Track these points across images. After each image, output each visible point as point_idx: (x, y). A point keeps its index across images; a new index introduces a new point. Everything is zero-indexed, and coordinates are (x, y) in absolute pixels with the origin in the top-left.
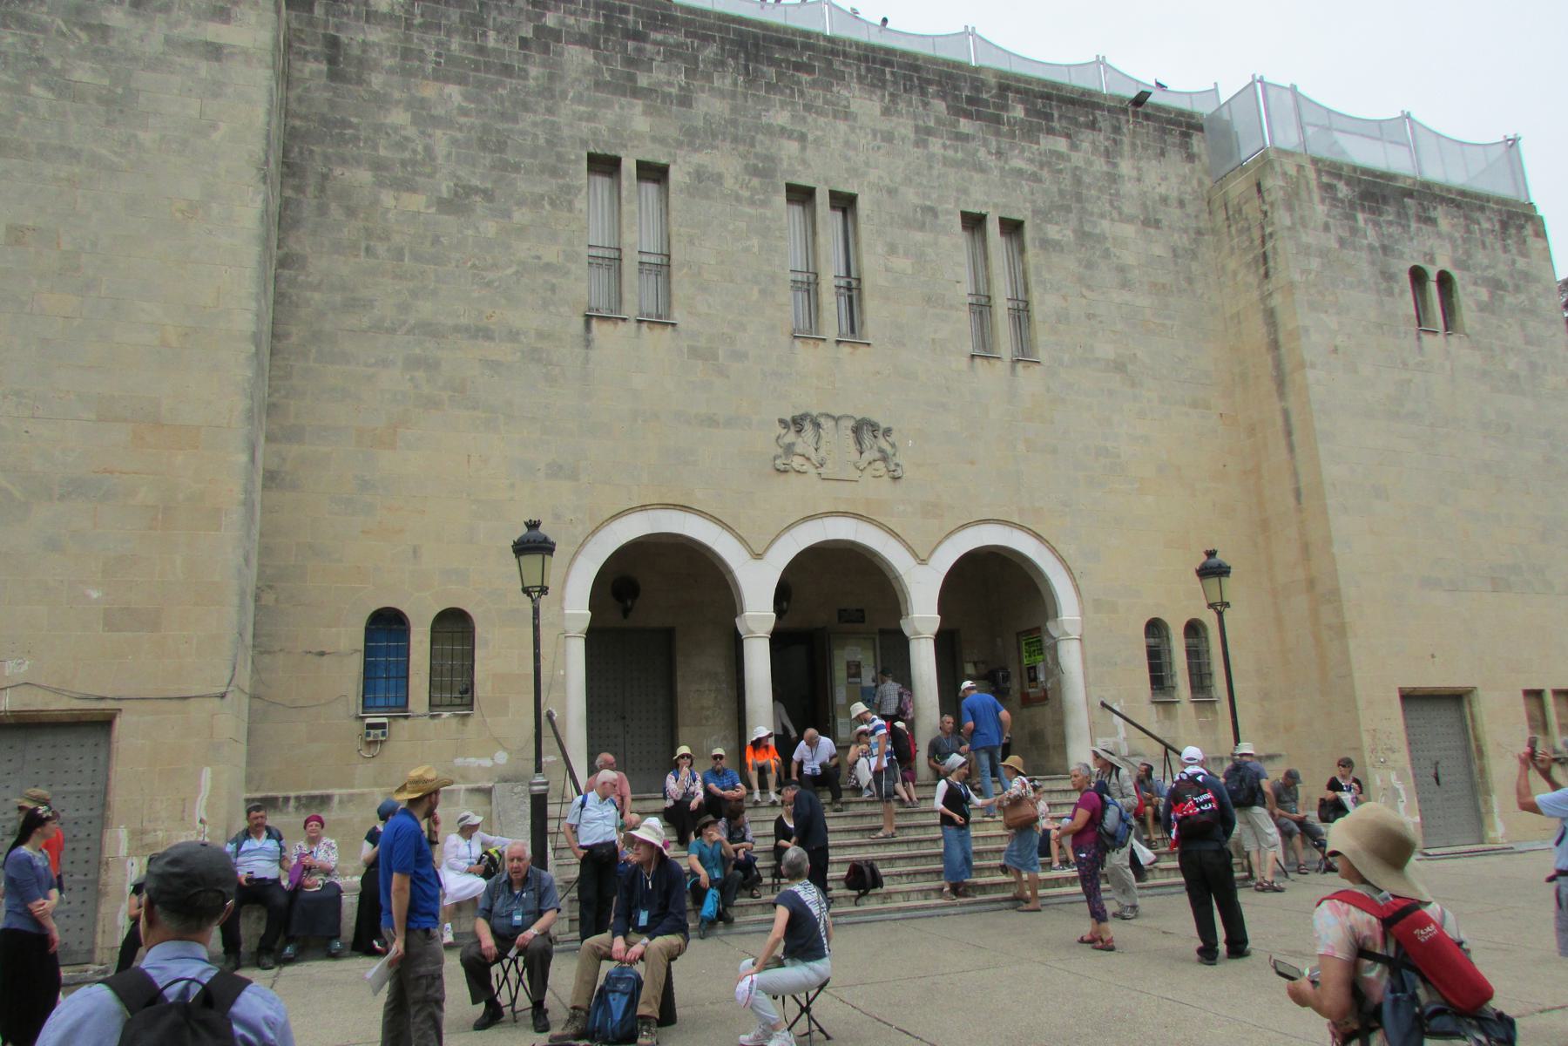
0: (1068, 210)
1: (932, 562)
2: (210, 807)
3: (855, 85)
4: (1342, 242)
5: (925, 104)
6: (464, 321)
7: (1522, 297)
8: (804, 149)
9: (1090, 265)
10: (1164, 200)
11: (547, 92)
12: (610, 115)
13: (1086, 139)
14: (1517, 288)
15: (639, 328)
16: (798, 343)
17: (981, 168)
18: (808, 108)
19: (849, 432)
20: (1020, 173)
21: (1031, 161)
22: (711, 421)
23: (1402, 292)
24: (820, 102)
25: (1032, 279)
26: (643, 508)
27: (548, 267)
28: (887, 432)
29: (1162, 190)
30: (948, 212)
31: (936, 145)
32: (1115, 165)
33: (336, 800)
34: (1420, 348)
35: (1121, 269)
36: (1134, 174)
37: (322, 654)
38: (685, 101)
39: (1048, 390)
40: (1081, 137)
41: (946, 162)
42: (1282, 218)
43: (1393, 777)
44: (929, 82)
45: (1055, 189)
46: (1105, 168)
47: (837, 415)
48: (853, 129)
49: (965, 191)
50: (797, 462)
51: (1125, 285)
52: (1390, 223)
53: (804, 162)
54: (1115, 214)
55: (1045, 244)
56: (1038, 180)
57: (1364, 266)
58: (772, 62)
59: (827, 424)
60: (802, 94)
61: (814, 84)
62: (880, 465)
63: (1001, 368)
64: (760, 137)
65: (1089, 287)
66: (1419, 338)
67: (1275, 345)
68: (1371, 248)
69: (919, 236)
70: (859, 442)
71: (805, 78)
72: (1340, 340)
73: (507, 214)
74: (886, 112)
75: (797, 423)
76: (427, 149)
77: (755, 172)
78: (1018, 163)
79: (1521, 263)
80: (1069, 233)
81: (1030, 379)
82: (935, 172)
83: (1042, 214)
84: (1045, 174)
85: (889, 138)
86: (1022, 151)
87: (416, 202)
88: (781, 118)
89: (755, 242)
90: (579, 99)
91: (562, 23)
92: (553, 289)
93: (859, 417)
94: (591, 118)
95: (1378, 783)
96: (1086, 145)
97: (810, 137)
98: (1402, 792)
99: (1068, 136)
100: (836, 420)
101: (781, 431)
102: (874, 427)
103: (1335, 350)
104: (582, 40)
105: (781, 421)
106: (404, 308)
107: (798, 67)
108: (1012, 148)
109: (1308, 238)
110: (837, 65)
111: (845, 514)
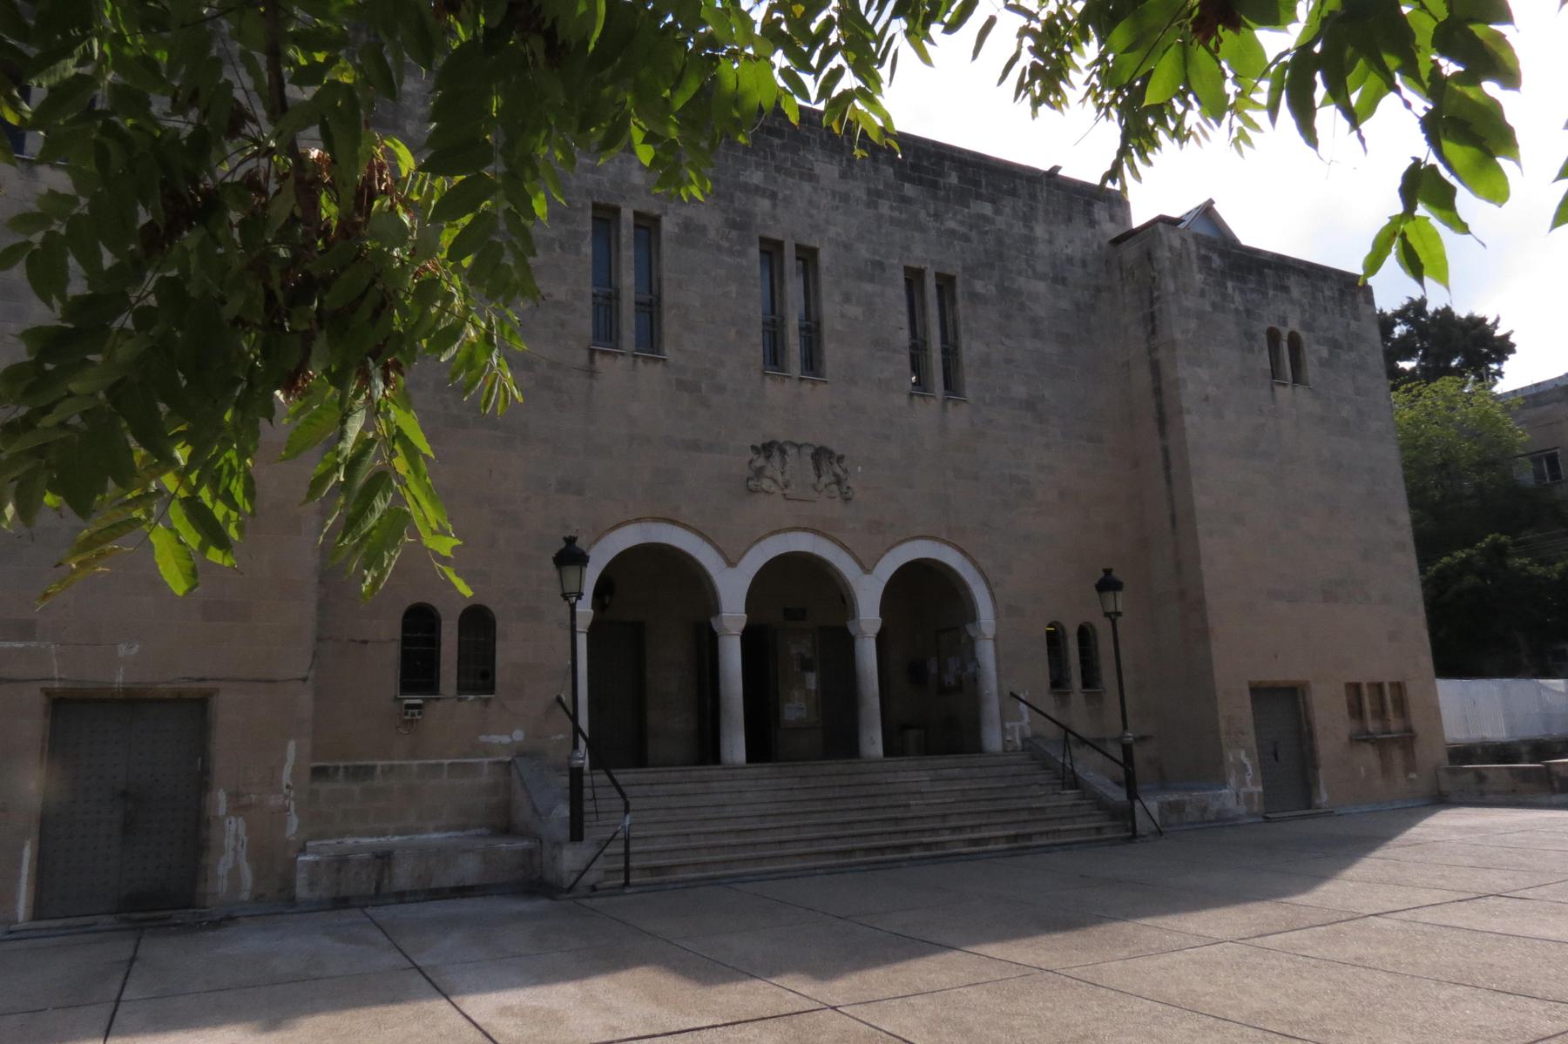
1: (875, 571)
2: (294, 776)
3: (817, 149)
4: (1214, 305)
5: (876, 170)
7: (1353, 354)
8: (774, 206)
10: (1070, 260)
13: (1007, 203)
14: (1351, 348)
15: (635, 363)
16: (768, 380)
17: (922, 229)
18: (778, 169)
19: (809, 459)
20: (953, 232)
21: (962, 223)
22: (695, 446)
23: (1261, 349)
24: (789, 164)
25: (962, 327)
26: (638, 520)
28: (841, 459)
29: (1069, 251)
31: (885, 208)
32: (1032, 229)
33: (379, 769)
34: (1274, 398)
35: (1034, 320)
36: (1047, 237)
37: (365, 642)
41: (893, 221)
42: (1169, 285)
46: (1023, 231)
47: (799, 442)
48: (815, 189)
49: (907, 248)
50: (766, 484)
51: (1037, 334)
53: (774, 218)
54: (1030, 272)
55: (974, 297)
56: (967, 239)
59: (791, 451)
60: (773, 156)
61: (783, 147)
62: (834, 487)
63: (934, 405)
64: (738, 194)
65: (1008, 336)
66: (1273, 389)
67: (1158, 391)
68: (1237, 311)
69: (869, 287)
70: (817, 468)
71: (777, 141)
72: (1211, 390)
74: (843, 176)
75: (767, 449)
77: (733, 225)
78: (951, 224)
79: (1354, 324)
80: (992, 288)
81: (959, 417)
82: (883, 231)
84: (973, 234)
85: (845, 198)
86: (955, 214)
88: (756, 177)
89: (733, 288)
92: (563, 325)
96: (1007, 210)
97: (780, 196)
99: (993, 202)
100: (799, 447)
101: (751, 455)
102: (830, 453)
103: (1207, 399)
105: (753, 447)
109: (1190, 302)
111: (805, 529)
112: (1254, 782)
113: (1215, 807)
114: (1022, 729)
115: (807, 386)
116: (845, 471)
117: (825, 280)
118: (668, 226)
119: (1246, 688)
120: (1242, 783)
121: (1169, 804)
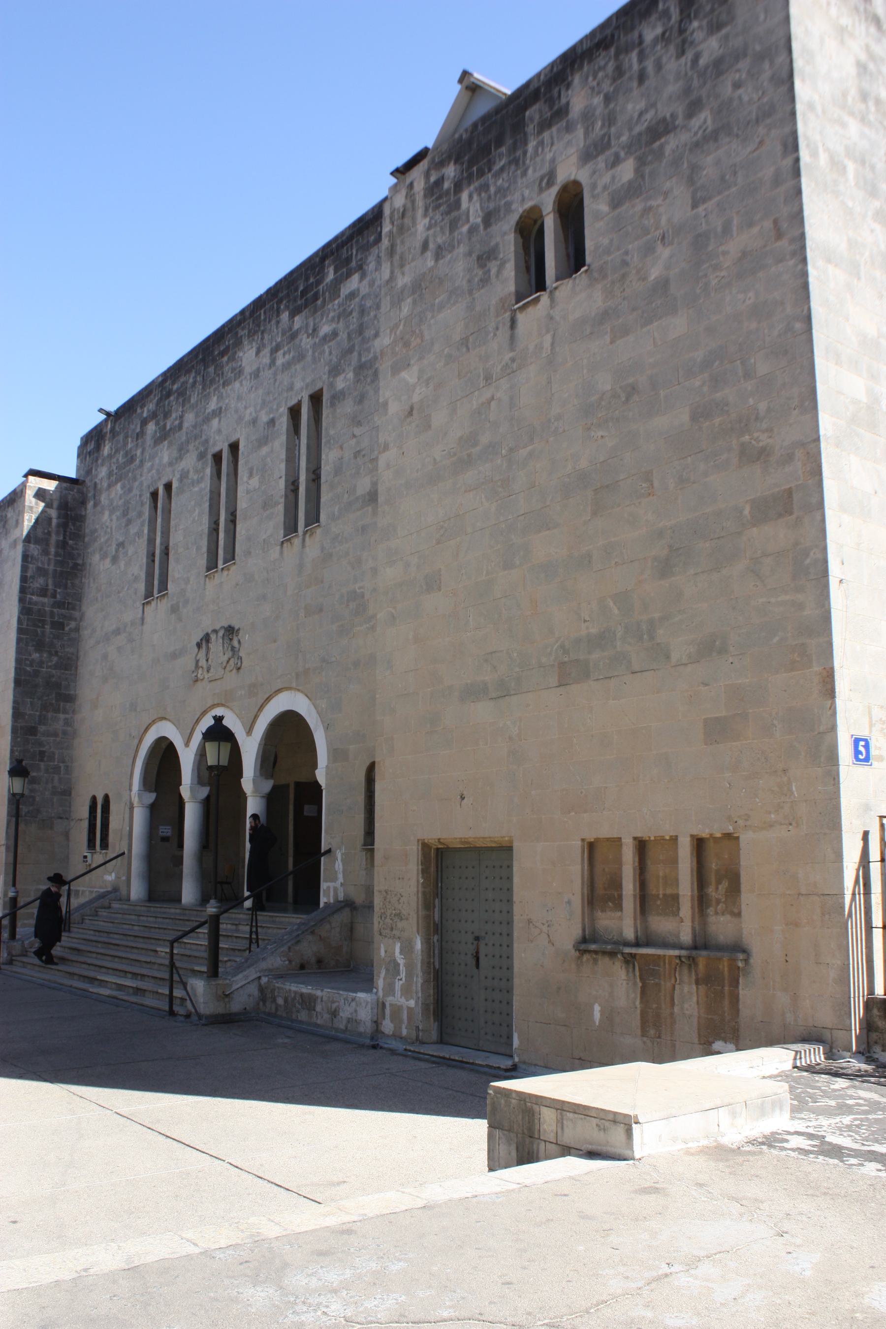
0: (350, 350)
6: (114, 627)
11: (142, 462)
12: (157, 460)
17: (301, 357)
21: (333, 320)
22: (174, 656)
26: (154, 722)
28: (239, 630)
30: (281, 415)
31: (280, 361)
38: (180, 427)
39: (323, 549)
44: (280, 302)
45: (345, 336)
47: (217, 628)
49: (291, 388)
52: (502, 169)
53: (219, 431)
57: (459, 266)
58: (214, 360)
59: (213, 637)
61: (227, 363)
65: (359, 424)
69: (265, 450)
71: (225, 359)
73: (126, 554)
74: (258, 352)
76: (111, 528)
78: (325, 329)
80: (351, 375)
81: (313, 546)
82: (277, 384)
83: (335, 371)
85: (256, 374)
90: (150, 460)
91: (149, 411)
93: (226, 626)
95: (383, 953)
98: (402, 968)
100: (215, 631)
107: (223, 354)
108: (322, 316)
110: (241, 333)
112: (407, 991)
113: (345, 1013)
114: (336, 890)
115: (225, 573)
116: (239, 642)
118: (175, 485)
119: (414, 850)
120: (390, 989)
121: (302, 995)
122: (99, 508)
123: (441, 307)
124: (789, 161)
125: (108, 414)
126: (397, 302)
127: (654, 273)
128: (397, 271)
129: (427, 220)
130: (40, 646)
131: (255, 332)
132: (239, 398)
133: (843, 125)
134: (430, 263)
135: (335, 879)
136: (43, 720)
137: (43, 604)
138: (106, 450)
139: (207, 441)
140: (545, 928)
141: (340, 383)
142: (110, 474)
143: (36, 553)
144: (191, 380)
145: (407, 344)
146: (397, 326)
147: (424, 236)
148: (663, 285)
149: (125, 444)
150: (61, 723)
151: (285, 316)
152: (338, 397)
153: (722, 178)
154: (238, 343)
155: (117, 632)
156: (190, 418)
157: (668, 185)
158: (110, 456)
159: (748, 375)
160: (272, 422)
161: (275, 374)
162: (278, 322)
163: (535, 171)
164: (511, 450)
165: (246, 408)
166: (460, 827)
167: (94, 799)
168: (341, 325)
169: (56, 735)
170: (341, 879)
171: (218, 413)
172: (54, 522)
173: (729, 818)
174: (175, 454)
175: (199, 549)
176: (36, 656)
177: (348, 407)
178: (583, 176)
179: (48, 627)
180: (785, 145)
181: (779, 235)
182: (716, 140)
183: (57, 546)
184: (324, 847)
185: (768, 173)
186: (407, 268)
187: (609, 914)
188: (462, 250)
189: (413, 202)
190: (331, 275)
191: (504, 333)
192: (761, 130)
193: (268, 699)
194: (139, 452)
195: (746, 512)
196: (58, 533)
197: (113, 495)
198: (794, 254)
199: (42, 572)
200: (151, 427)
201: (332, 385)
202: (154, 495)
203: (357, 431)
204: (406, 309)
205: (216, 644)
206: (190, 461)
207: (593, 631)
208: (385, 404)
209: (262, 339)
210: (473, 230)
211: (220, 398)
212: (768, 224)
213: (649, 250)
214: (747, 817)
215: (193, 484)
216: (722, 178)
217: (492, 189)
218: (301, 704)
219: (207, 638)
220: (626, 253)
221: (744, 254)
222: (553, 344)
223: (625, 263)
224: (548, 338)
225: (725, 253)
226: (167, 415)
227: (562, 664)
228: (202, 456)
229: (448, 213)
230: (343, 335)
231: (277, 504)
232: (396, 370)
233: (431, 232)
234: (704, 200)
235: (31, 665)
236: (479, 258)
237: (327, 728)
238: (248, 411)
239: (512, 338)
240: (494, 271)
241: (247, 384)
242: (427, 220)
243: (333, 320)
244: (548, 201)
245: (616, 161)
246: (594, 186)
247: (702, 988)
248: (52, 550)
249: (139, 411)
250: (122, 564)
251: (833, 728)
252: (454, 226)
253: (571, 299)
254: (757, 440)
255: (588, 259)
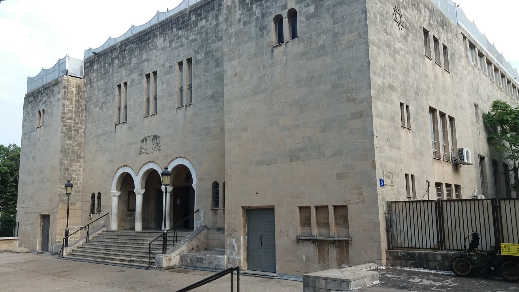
0: (203, 46)
6: (102, 132)
9: (207, 63)
11: (113, 74)
17: (182, 46)
20: (192, 40)
22: (131, 144)
26: (121, 167)
27: (112, 116)
30: (175, 65)
35: (216, 60)
38: (130, 63)
39: (194, 112)
40: (209, 15)
43: (234, 241)
49: (179, 56)
53: (148, 67)
55: (198, 62)
57: (253, 29)
58: (144, 41)
59: (148, 139)
61: (150, 43)
65: (207, 72)
69: (168, 76)
71: (149, 41)
72: (237, 70)
73: (107, 106)
75: (142, 141)
78: (192, 37)
80: (203, 55)
83: (197, 52)
85: (163, 49)
87: (98, 109)
94: (117, 76)
95: (228, 243)
98: (236, 247)
104: (118, 57)
106: (96, 132)
107: (149, 39)
108: (191, 32)
110: (156, 33)
114: (201, 223)
116: (160, 141)
117: (158, 79)
122: (92, 88)
123: (246, 42)
124: (363, 16)
125: (96, 54)
126: (230, 37)
127: (320, 43)
128: (229, 28)
129: (240, 12)
130: (70, 138)
131: (162, 34)
132: (156, 56)
133: (376, 4)
134: (242, 27)
135: (200, 219)
136: (71, 166)
137: (71, 123)
138: (95, 67)
139: (142, 70)
140: (286, 233)
141: (199, 57)
142: (98, 76)
143: (68, 104)
144: (134, 47)
145: (233, 52)
146: (230, 45)
147: (239, 17)
148: (323, 47)
149: (104, 66)
150: (78, 166)
151: (175, 30)
152: (198, 62)
153: (343, 17)
154: (155, 36)
155: (103, 134)
156: (134, 61)
157: (325, 16)
158: (97, 70)
159: (350, 77)
160: (171, 67)
161: (172, 50)
162: (172, 32)
163: (280, 3)
164: (272, 91)
165: (159, 60)
166: (255, 202)
167: (93, 194)
168: (198, 37)
169: (76, 171)
170: (203, 220)
171: (147, 60)
172: (74, 92)
173: (344, 201)
174: (128, 73)
175: (140, 107)
176: (68, 142)
177: (202, 66)
178: (297, 8)
179: (73, 131)
180: (362, 11)
181: (360, 37)
182: (341, 5)
183: (76, 102)
184: (195, 209)
185: (357, 18)
186: (233, 27)
187: (306, 228)
188: (253, 24)
189: (235, 4)
190: (193, 18)
191: (269, 54)
192: (355, 5)
193: (173, 160)
194: (111, 70)
195: (349, 116)
196: (76, 97)
197: (99, 84)
198: (364, 43)
199: (70, 111)
200: (116, 61)
201: (195, 57)
202: (119, 86)
203: (206, 74)
204: (233, 40)
205: (149, 141)
206: (135, 76)
207: (300, 147)
208: (226, 71)
209: (165, 36)
210: (257, 18)
211: (148, 55)
212: (357, 33)
213: (319, 35)
214: (350, 201)
215: (137, 84)
216: (343, 17)
217: (264, 6)
218: (186, 163)
219: (145, 139)
220: (311, 35)
221: (349, 41)
222: (286, 60)
223: (311, 38)
224: (285, 58)
225: (343, 40)
226: (124, 58)
227: (290, 156)
228: (140, 75)
229: (248, 11)
230: (199, 40)
231: (174, 95)
232: (230, 60)
233: (242, 16)
234: (337, 23)
235: (67, 145)
236: (260, 28)
237: (196, 170)
238: (161, 61)
239: (272, 56)
240: (265, 34)
241: (159, 52)
242: (240, 12)
243: (195, 34)
244: (285, 14)
245: (308, 5)
246: (300, 12)
247: (338, 249)
248: (74, 103)
249: (110, 55)
250: (105, 110)
251: (375, 177)
252: (250, 16)
253: (293, 47)
254: (352, 96)
255: (298, 35)
